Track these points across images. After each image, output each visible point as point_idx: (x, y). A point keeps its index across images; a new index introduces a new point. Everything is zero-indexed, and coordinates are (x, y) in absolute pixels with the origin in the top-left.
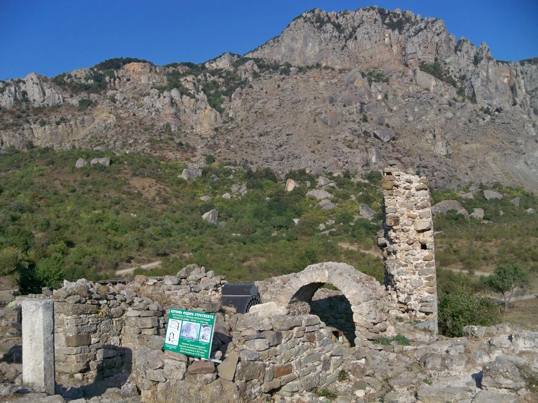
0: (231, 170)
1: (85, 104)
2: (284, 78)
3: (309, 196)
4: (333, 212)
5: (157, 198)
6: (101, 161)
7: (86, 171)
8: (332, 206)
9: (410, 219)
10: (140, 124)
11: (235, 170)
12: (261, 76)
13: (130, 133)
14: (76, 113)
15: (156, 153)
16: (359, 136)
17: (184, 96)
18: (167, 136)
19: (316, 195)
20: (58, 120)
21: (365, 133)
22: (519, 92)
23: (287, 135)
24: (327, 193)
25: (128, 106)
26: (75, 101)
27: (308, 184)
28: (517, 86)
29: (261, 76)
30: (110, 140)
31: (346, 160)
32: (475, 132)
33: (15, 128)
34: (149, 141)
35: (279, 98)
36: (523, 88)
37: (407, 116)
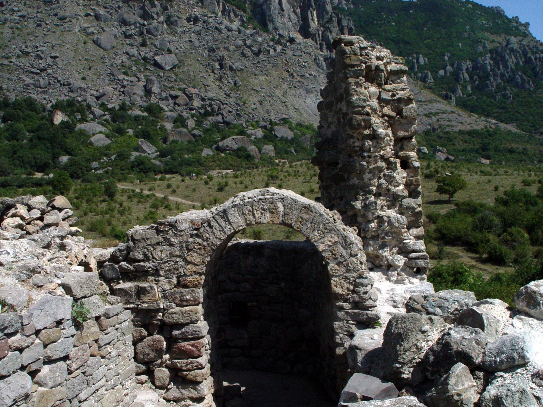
3: (81, 130)
4: (107, 147)
8: (108, 142)
9: (386, 118)
16: (136, 62)
21: (145, 59)
22: (312, 24)
23: (51, 57)
27: (79, 117)
28: (310, 17)
31: (122, 90)
32: (265, 63)
35: (41, 12)
36: (316, 20)
37: (191, 41)
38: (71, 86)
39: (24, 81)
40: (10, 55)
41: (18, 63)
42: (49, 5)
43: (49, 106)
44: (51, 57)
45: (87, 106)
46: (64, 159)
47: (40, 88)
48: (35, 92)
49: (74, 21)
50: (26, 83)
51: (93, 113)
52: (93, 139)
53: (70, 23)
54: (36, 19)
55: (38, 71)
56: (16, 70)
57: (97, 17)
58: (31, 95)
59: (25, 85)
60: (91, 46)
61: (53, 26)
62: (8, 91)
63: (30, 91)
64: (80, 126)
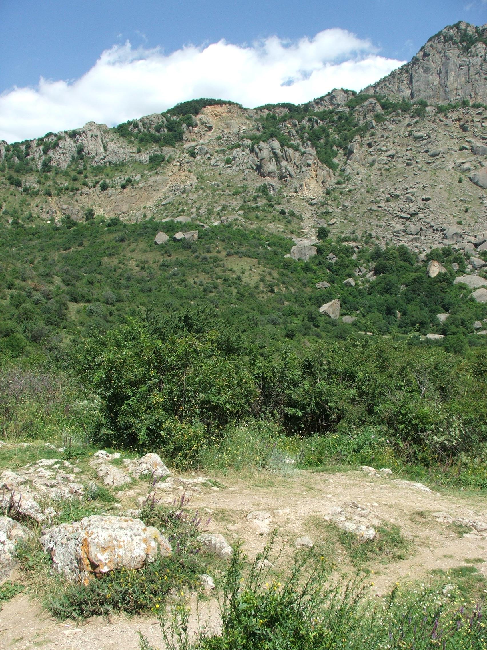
0: (353, 248)
1: (156, 161)
2: (417, 122)
3: (460, 283)
5: (261, 287)
6: (188, 235)
7: (164, 249)
10: (229, 186)
11: (358, 248)
12: (386, 120)
13: (217, 197)
14: (146, 172)
15: (251, 224)
17: (286, 148)
18: (265, 201)
19: (467, 283)
20: (124, 182)
23: (423, 200)
24: (483, 279)
25: (213, 162)
26: (144, 157)
27: (456, 267)
29: (386, 120)
30: (192, 208)
33: (71, 193)
34: (241, 208)
35: (411, 150)
38: (445, 232)
39: (394, 228)
40: (378, 199)
41: (386, 208)
42: (419, 142)
43: (423, 256)
44: (423, 200)
45: (465, 255)
46: (442, 317)
47: (411, 234)
48: (406, 240)
49: (447, 156)
50: (395, 230)
51: (471, 263)
52: (475, 294)
53: (443, 160)
54: (405, 158)
55: (409, 216)
56: (384, 216)
57: (474, 151)
58: (402, 243)
59: (395, 232)
60: (467, 185)
61: (424, 164)
62: (378, 239)
63: (400, 239)
64: (459, 279)
